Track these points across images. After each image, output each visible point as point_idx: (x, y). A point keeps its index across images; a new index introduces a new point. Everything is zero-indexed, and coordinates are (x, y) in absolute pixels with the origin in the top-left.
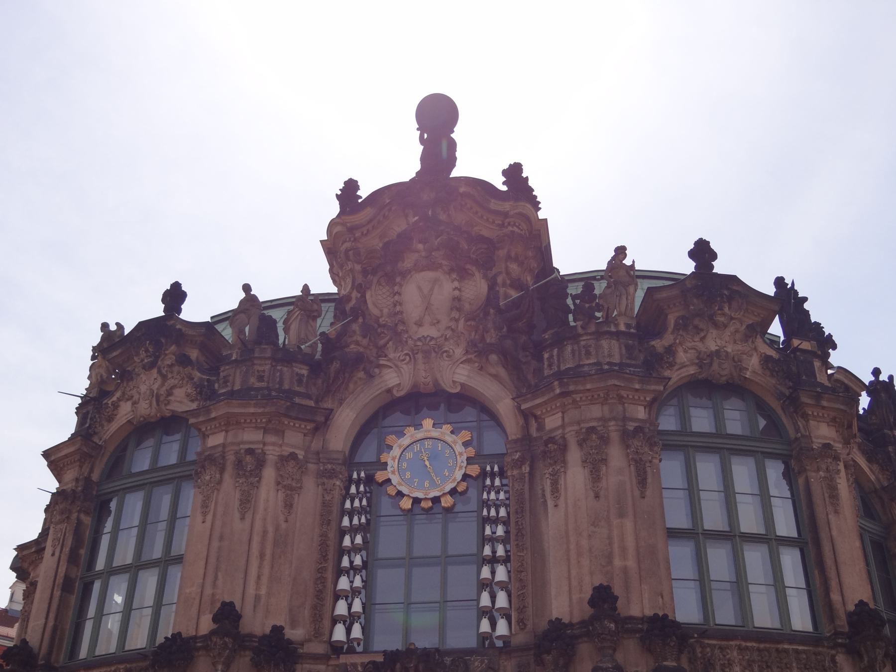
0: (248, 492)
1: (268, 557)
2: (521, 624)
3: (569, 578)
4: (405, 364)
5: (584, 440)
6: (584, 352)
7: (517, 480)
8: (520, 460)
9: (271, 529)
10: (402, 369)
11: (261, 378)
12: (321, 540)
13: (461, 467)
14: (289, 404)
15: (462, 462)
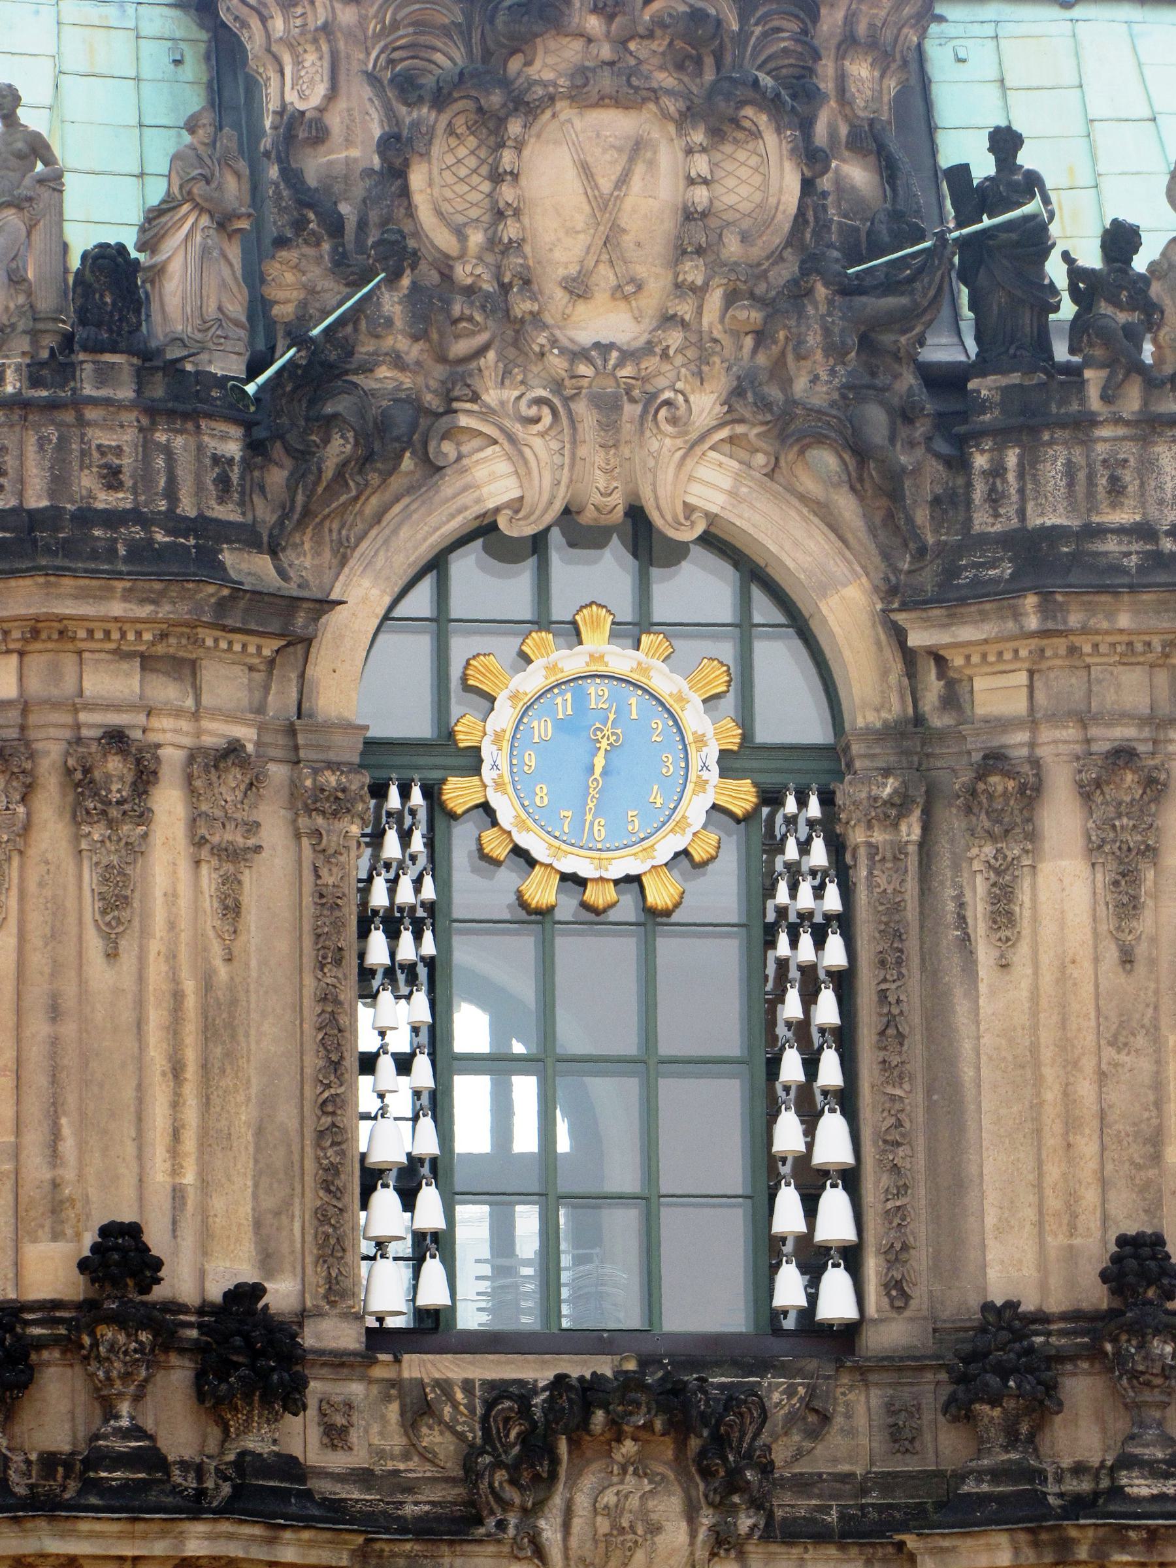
0: (122, 873)
1: (191, 1072)
2: (894, 1293)
3: (1039, 1186)
4: (542, 435)
5: (1098, 783)
6: (1104, 481)
7: (883, 859)
8: (897, 800)
9: (189, 986)
10: (527, 451)
11: (112, 478)
12: (323, 1011)
13: (702, 784)
14: (226, 592)
15: (705, 767)
